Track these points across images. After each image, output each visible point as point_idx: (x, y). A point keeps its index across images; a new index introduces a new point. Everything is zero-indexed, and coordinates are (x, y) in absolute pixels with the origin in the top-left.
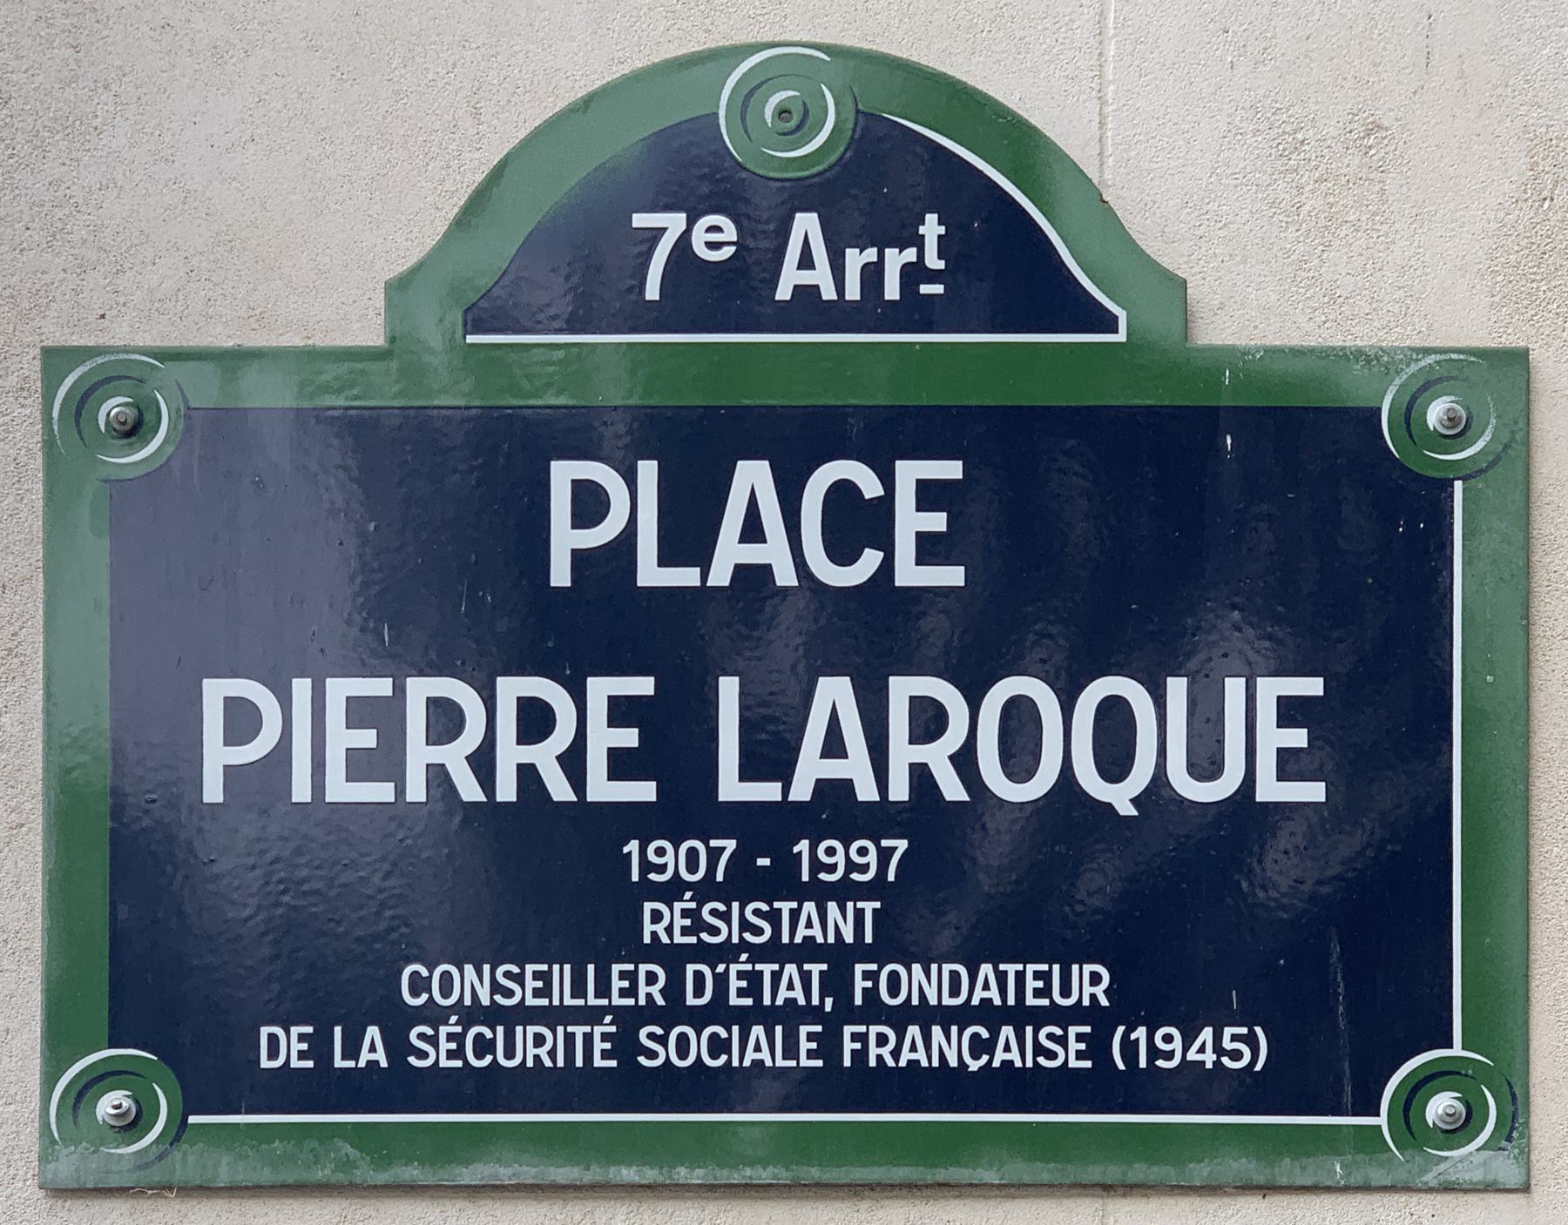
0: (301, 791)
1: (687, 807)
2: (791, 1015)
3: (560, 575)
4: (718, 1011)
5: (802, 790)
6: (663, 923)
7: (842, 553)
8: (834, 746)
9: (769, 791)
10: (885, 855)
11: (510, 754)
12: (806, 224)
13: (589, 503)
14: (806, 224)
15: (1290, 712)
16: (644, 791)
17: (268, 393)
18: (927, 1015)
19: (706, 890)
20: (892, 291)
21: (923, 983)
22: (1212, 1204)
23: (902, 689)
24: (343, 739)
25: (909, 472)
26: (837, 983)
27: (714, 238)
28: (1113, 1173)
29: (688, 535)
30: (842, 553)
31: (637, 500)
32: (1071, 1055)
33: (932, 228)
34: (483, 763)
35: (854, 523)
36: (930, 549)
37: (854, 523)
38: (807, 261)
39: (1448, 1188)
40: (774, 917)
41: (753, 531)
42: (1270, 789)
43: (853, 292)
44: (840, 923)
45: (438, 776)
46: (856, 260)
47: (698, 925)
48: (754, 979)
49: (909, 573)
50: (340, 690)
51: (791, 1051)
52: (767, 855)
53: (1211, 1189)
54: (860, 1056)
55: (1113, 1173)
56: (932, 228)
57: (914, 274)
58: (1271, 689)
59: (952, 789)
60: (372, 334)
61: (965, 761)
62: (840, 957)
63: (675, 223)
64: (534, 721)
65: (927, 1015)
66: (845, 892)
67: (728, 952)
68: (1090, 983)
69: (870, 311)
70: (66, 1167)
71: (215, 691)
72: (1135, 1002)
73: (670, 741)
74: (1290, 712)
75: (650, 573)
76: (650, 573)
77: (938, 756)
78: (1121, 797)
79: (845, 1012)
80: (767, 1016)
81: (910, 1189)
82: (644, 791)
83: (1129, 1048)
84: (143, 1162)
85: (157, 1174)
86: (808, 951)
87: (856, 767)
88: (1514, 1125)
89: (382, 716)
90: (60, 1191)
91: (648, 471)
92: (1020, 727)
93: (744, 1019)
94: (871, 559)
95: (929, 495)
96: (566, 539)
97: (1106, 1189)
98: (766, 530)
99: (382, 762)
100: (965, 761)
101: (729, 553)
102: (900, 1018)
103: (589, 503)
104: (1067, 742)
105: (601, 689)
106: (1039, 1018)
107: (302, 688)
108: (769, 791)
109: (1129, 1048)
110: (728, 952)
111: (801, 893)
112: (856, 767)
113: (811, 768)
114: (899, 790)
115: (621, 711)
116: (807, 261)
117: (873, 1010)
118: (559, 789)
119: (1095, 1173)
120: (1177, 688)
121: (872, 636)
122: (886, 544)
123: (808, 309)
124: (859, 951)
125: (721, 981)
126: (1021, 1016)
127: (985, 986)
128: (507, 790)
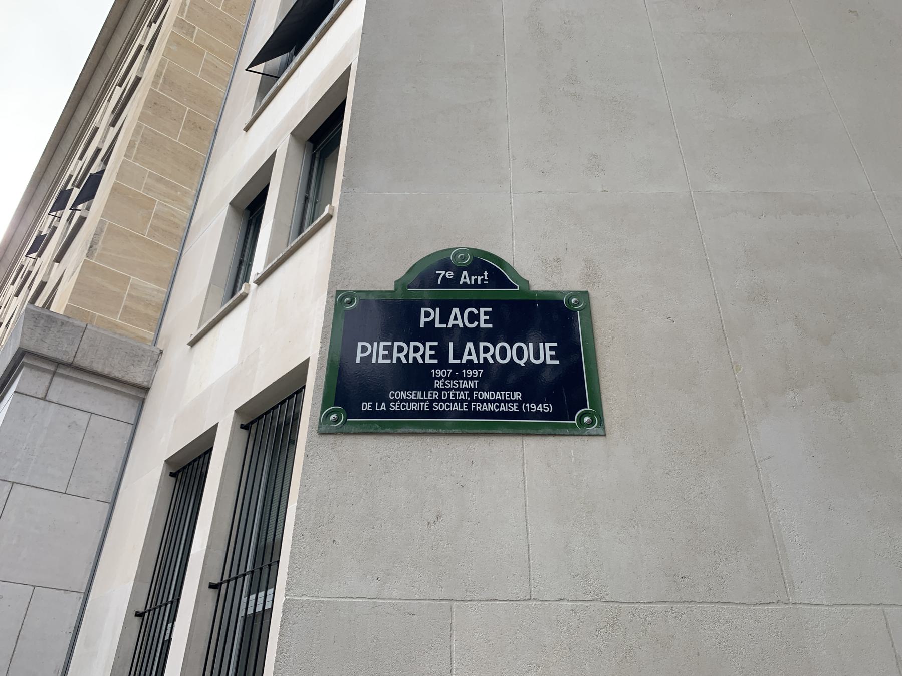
0: (374, 361)
1: (443, 363)
2: (462, 401)
3: (422, 326)
4: (448, 400)
5: (464, 361)
6: (438, 384)
7: (471, 322)
8: (470, 354)
9: (458, 361)
10: (479, 372)
11: (412, 355)
12: (465, 273)
13: (427, 315)
14: (465, 273)
15: (551, 348)
16: (436, 361)
17: (371, 298)
18: (487, 401)
19: (446, 378)
20: (479, 283)
21: (487, 395)
22: (544, 438)
23: (482, 344)
24: (382, 352)
25: (482, 310)
26: (471, 395)
27: (450, 275)
28: (524, 431)
29: (444, 319)
30: (471, 322)
31: (435, 314)
32: (515, 409)
33: (486, 274)
34: (407, 356)
35: (473, 318)
36: (486, 322)
37: (473, 318)
38: (465, 278)
39: (590, 435)
40: (459, 383)
41: (455, 319)
42: (549, 361)
43: (473, 283)
44: (471, 384)
45: (399, 358)
46: (473, 278)
47: (445, 384)
48: (455, 394)
49: (482, 325)
50: (382, 344)
51: (462, 407)
52: (458, 372)
53: (543, 435)
54: (475, 408)
55: (524, 431)
56: (486, 274)
57: (482, 280)
58: (548, 345)
59: (491, 361)
60: (392, 289)
61: (493, 356)
62: (471, 390)
63: (443, 273)
64: (417, 349)
65: (487, 401)
66: (472, 379)
67: (450, 389)
68: (518, 395)
69: (476, 285)
70: (323, 429)
71: (360, 344)
72: (525, 399)
73: (440, 353)
74: (551, 348)
75: (438, 325)
76: (438, 325)
77: (488, 355)
78: (522, 363)
79: (472, 400)
80: (457, 401)
81: (485, 434)
82: (436, 361)
83: (526, 408)
84: (341, 426)
85: (340, 430)
86: (465, 389)
87: (474, 357)
88: (601, 423)
89: (390, 349)
90: (321, 433)
91: (438, 310)
92: (503, 352)
93: (453, 401)
94: (476, 323)
95: (486, 313)
96: (423, 320)
97: (523, 434)
98: (458, 319)
99: (390, 356)
100: (493, 356)
101: (451, 322)
102: (482, 401)
103: (427, 315)
104: (512, 353)
105: (428, 344)
106: (508, 402)
107: (375, 344)
108: (458, 361)
109: (526, 408)
110: (450, 389)
111: (464, 379)
112: (474, 357)
113: (466, 357)
114: (481, 361)
115: (432, 348)
116: (465, 278)
117: (477, 400)
118: (420, 361)
119: (521, 431)
120: (531, 344)
121: (475, 335)
122: (479, 321)
123: (465, 285)
124: (475, 389)
125: (449, 394)
126: (505, 401)
127: (498, 395)
128: (411, 361)
